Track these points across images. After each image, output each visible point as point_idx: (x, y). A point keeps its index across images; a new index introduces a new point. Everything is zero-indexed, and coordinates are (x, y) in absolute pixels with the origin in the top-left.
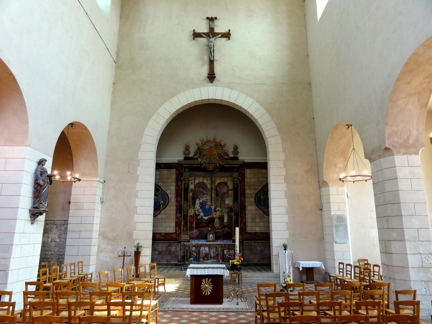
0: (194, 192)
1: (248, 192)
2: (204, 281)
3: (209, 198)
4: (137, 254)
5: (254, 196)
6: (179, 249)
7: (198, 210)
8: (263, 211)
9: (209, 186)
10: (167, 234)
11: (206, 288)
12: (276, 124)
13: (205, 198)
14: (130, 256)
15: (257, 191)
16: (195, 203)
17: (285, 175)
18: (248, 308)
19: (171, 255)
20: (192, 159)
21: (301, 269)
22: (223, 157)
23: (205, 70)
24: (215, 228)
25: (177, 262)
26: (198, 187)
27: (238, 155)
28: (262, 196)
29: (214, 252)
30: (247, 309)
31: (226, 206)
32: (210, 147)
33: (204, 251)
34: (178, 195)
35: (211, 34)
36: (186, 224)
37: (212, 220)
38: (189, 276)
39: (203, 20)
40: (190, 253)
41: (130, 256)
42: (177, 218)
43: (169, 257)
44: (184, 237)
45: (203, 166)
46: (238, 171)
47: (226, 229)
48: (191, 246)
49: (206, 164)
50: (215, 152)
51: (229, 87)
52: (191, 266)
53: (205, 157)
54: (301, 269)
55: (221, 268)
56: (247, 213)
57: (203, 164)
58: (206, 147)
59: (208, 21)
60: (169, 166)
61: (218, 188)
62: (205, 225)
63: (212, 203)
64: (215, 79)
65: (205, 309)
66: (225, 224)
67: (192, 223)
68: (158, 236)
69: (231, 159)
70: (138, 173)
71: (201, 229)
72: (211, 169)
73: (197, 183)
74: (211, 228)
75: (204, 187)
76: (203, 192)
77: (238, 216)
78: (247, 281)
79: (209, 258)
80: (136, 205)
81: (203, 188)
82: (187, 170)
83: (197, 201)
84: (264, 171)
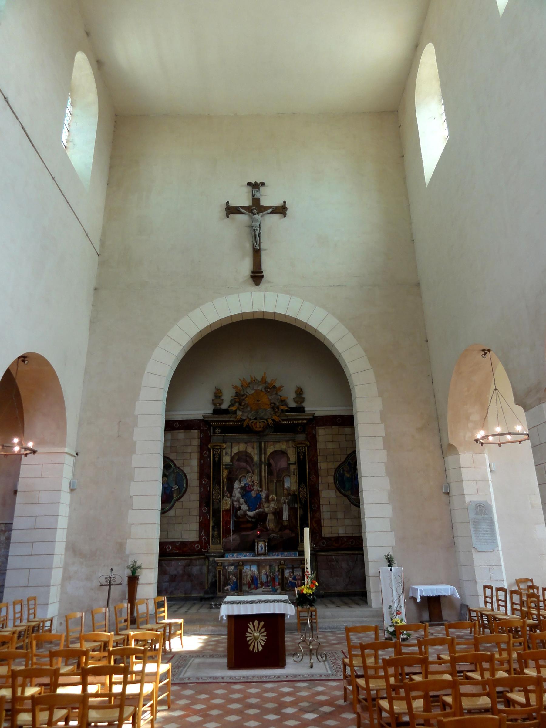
0: (229, 468)
1: (322, 466)
2: (251, 625)
3: (256, 478)
4: (133, 580)
5: (332, 472)
6: (205, 569)
7: (238, 501)
8: (349, 499)
9: (256, 459)
10: (184, 544)
11: (256, 638)
12: (365, 351)
13: (249, 479)
14: (120, 584)
15: (337, 464)
16: (232, 487)
17: (384, 435)
18: (330, 672)
20: (226, 411)
21: (419, 600)
22: (278, 408)
23: (246, 267)
24: (267, 530)
25: (202, 595)
26: (238, 460)
27: (304, 405)
28: (345, 473)
29: (266, 574)
30: (328, 675)
31: (285, 492)
32: (257, 392)
33: (250, 573)
34: (203, 474)
35: (256, 207)
36: (217, 525)
37: (262, 517)
38: (225, 618)
39: (242, 186)
40: (225, 578)
41: (120, 584)
42: (201, 514)
43: (188, 585)
44: (214, 548)
45: (245, 424)
46: (304, 431)
47: (287, 531)
48: (226, 564)
49: (250, 419)
50: (265, 399)
51: (287, 292)
52: (229, 598)
53: (249, 409)
54: (419, 600)
55: (281, 601)
56: (321, 502)
57: (244, 420)
58: (250, 391)
59: (250, 188)
60: (186, 425)
61: (271, 461)
62: (249, 525)
63: (261, 487)
64: (264, 280)
65: (254, 677)
66: (286, 523)
67: (227, 523)
68: (169, 548)
69: (293, 410)
70: (135, 439)
71: (244, 533)
72: (258, 429)
73: (236, 454)
74: (261, 531)
75: (248, 459)
76: (245, 469)
77: (307, 509)
78: (326, 625)
79: (259, 585)
80: (131, 494)
81: (246, 462)
82: (218, 431)
83: (236, 485)
84: (347, 430)
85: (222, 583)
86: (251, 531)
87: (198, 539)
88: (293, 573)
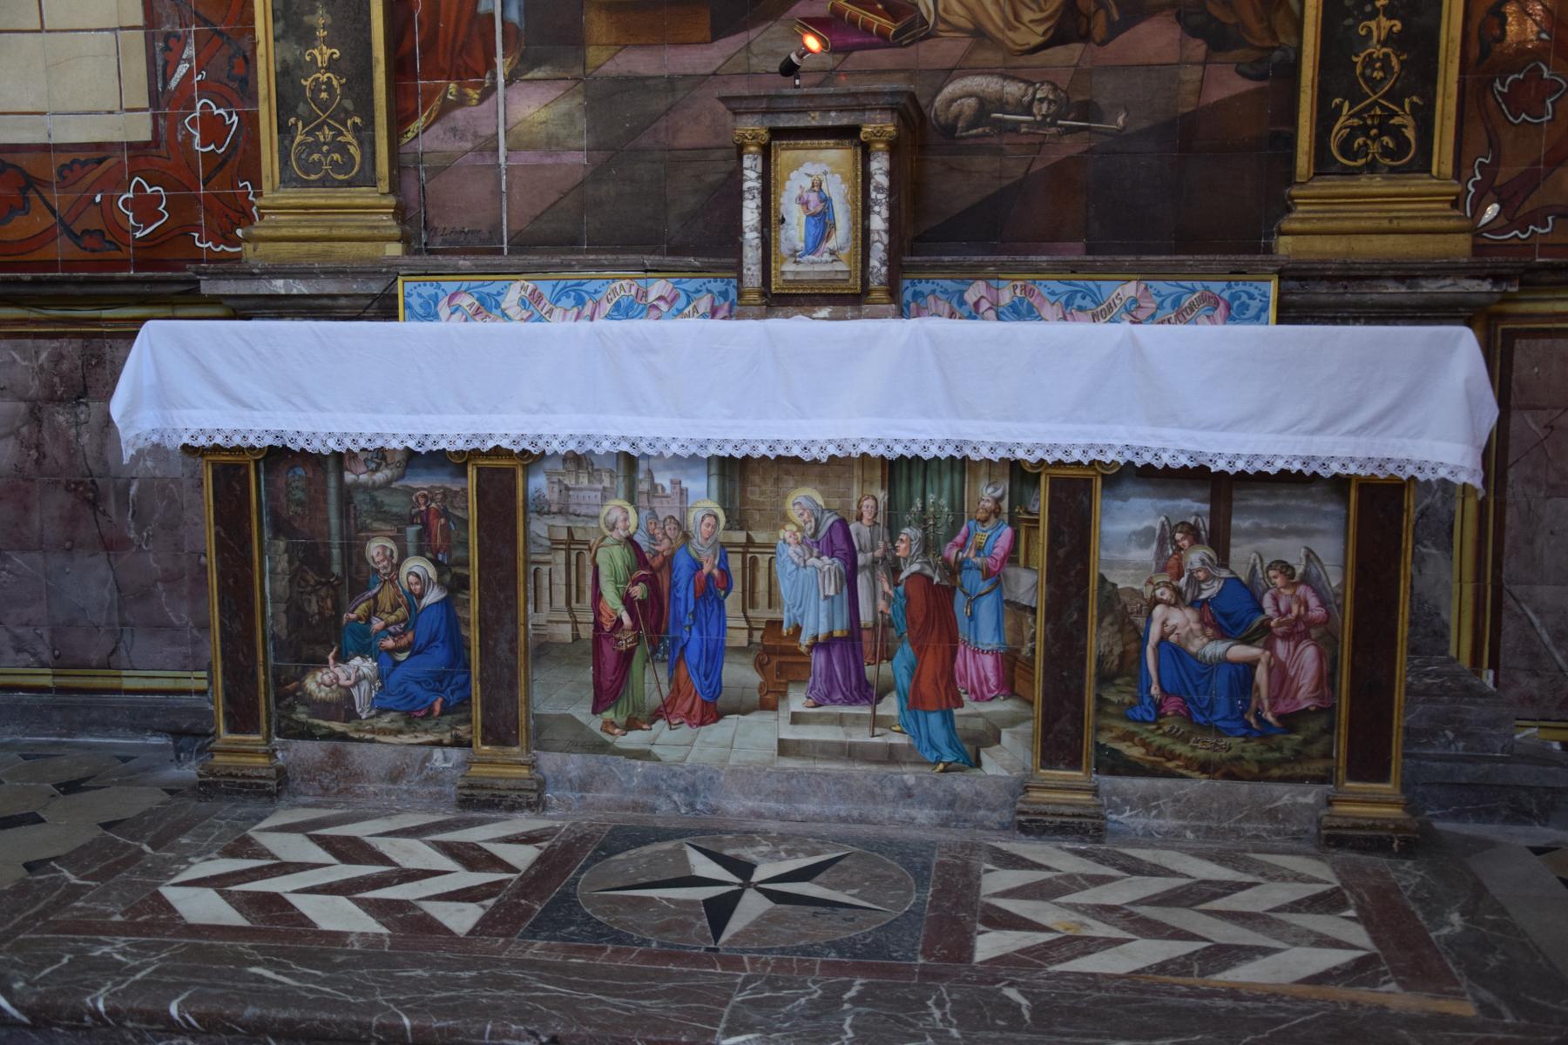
19: (112, 545)
29: (836, 541)
40: (310, 558)
43: (89, 584)
79: (739, 674)
85: (271, 617)
86: (717, 34)
87: (140, 129)
88: (1219, 541)
